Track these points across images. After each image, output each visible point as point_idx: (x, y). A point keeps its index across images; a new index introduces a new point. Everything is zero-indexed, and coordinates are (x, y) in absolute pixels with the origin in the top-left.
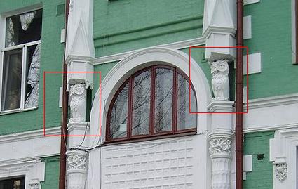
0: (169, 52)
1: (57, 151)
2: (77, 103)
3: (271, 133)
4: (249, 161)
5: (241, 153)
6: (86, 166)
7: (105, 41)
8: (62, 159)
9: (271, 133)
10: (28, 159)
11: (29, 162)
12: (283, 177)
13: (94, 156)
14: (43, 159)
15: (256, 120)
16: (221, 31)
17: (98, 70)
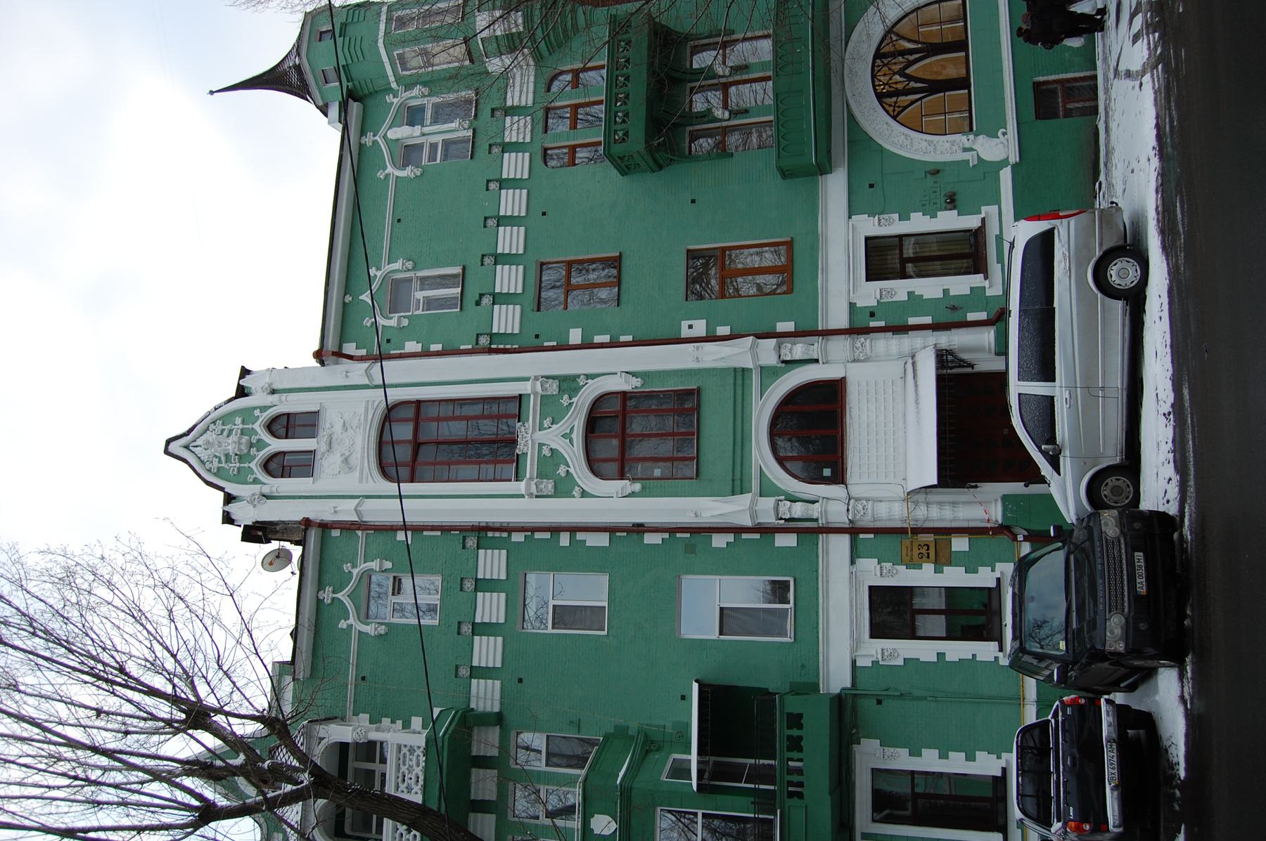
0: (762, 409)
1: (845, 539)
2: (798, 510)
3: (852, 306)
4: (872, 324)
5: (867, 331)
6: (868, 500)
7: (738, 483)
8: (853, 531)
9: (852, 306)
10: (851, 583)
11: (853, 578)
12: (891, 292)
13: (856, 491)
14: (853, 562)
15: (839, 319)
16: (753, 347)
17: (767, 489)
